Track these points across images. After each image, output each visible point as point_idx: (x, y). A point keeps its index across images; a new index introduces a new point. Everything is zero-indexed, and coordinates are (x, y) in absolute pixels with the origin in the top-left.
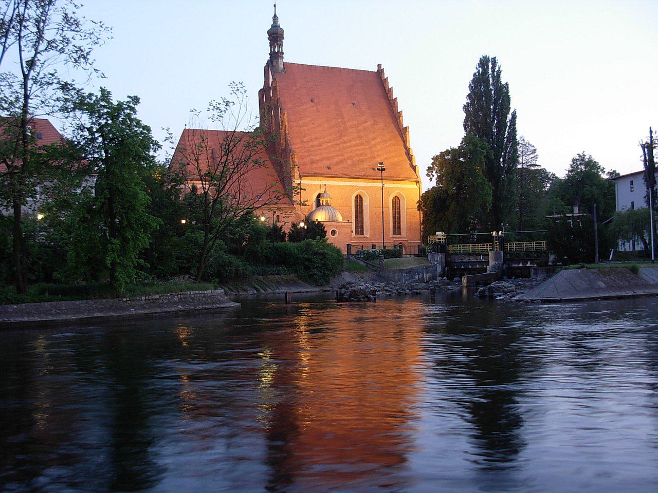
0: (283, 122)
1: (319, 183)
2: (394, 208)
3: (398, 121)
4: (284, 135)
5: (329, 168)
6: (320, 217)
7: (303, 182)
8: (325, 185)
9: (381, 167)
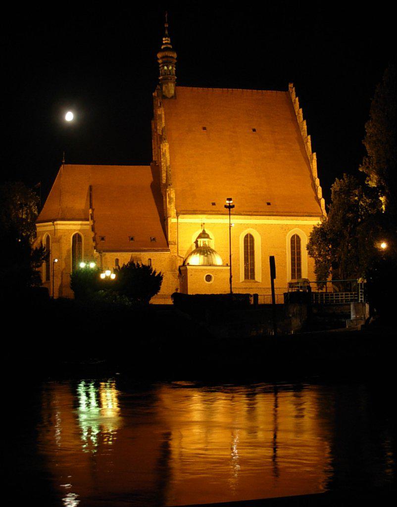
0: (164, 154)
1: (201, 222)
2: (293, 248)
3: (306, 147)
4: (165, 168)
5: (214, 204)
6: (196, 260)
7: (180, 220)
8: (204, 224)
9: (229, 204)
